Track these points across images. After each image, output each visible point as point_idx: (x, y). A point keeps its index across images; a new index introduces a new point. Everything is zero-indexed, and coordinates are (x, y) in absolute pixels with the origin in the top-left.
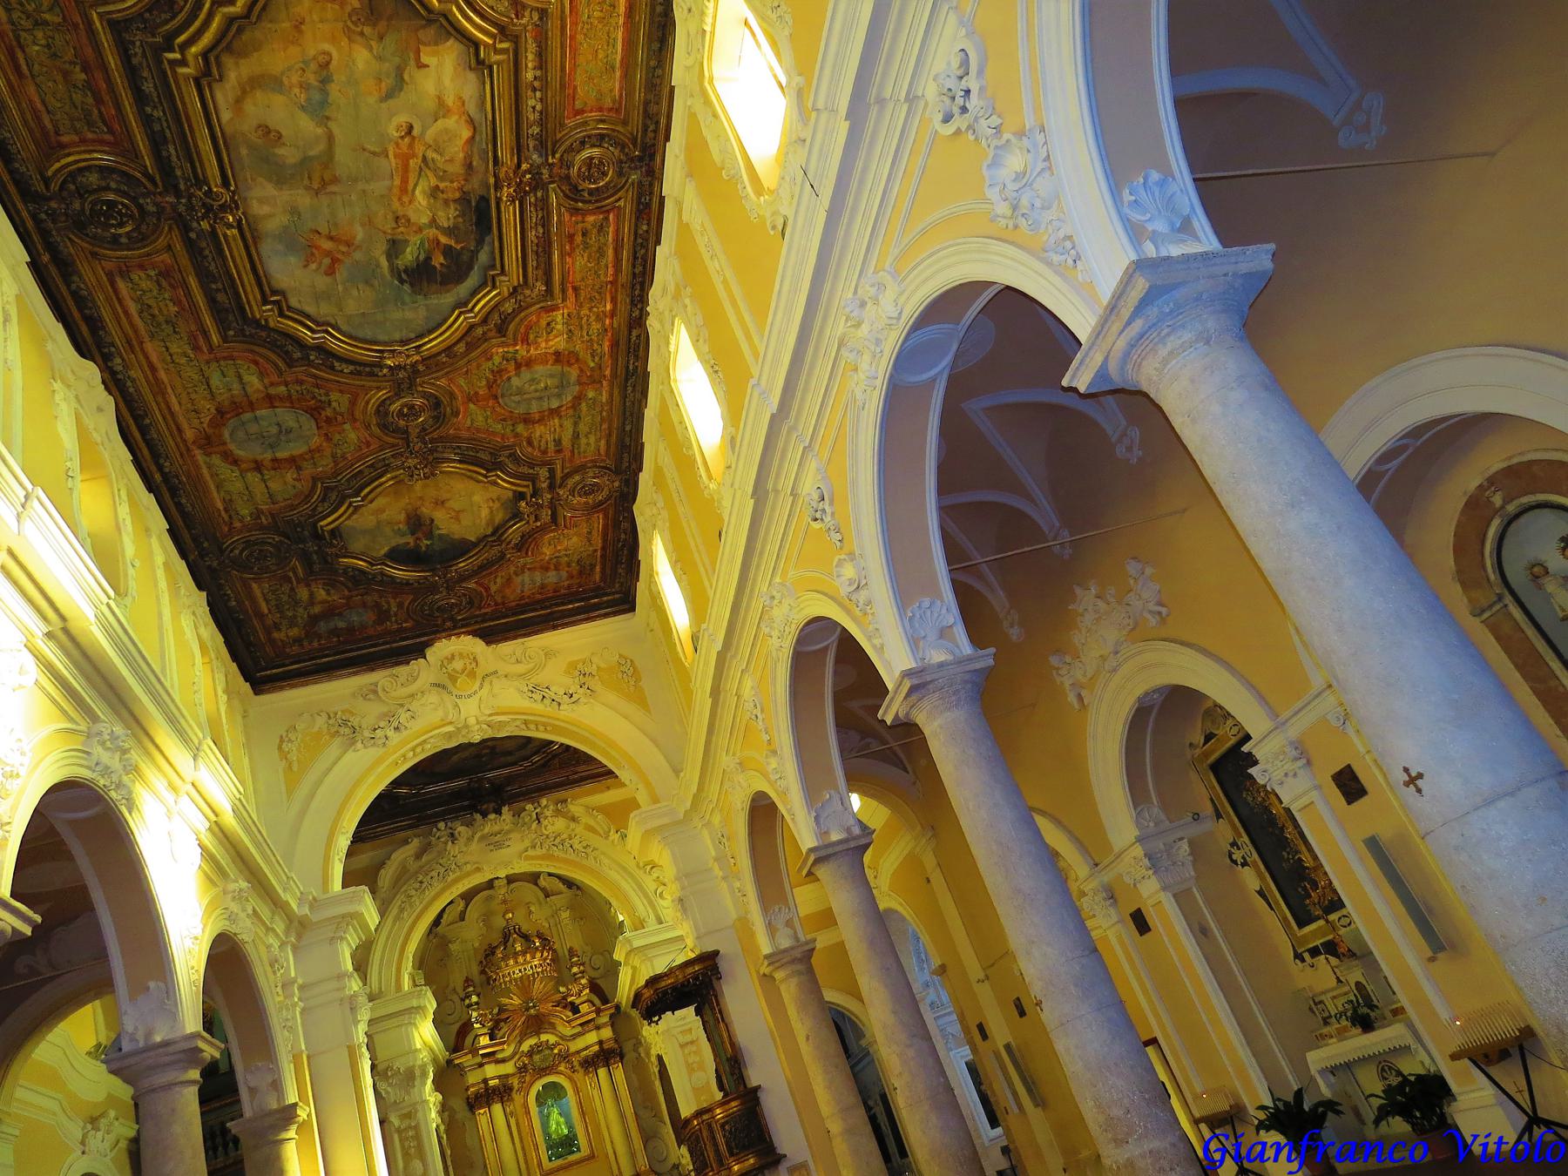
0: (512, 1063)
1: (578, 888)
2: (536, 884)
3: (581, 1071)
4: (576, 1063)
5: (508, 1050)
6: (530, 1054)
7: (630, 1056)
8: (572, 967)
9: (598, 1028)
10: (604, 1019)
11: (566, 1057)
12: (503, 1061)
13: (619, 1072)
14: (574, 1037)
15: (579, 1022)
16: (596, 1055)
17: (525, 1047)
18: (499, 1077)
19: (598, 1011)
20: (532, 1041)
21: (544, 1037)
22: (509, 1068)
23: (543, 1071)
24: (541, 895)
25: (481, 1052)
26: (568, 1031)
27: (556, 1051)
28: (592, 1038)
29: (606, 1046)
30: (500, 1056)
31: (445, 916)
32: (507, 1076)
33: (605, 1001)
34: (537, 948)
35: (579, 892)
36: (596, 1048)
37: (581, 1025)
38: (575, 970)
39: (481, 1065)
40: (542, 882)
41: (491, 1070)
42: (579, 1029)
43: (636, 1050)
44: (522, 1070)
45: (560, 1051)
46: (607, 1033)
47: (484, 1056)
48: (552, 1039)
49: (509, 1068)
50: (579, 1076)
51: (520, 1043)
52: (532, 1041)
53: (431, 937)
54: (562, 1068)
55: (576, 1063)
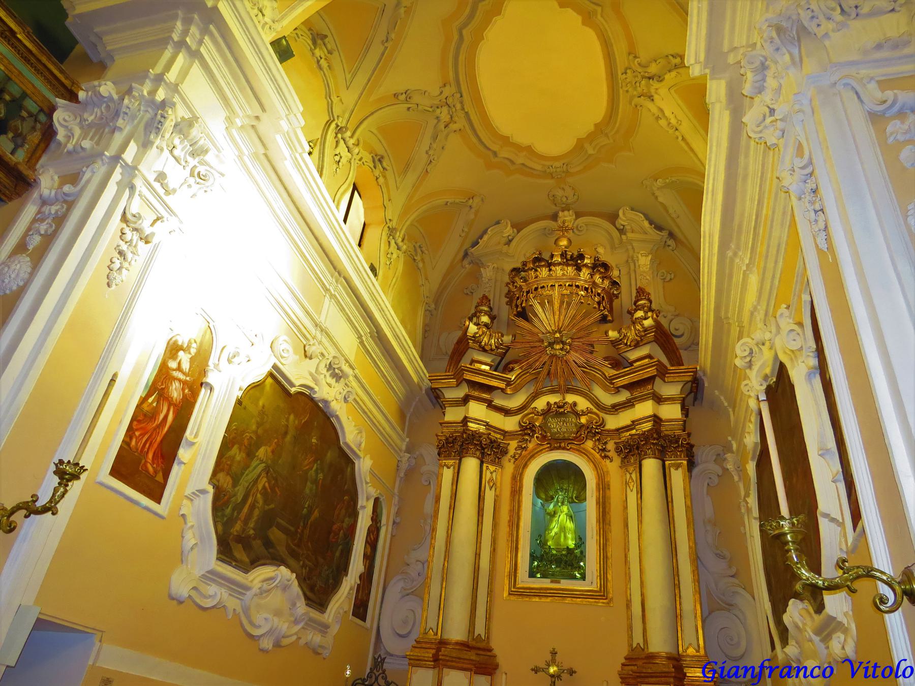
0: (519, 417)
1: (671, 235)
2: (615, 225)
3: (617, 460)
4: (611, 446)
5: (515, 402)
6: (547, 412)
7: (703, 454)
8: (636, 310)
9: (659, 400)
10: (671, 390)
11: (596, 431)
12: (506, 412)
13: (678, 477)
14: (616, 408)
15: (625, 380)
16: (646, 436)
17: (540, 404)
18: (487, 424)
19: (662, 373)
20: (553, 399)
21: (570, 398)
22: (510, 424)
23: (556, 443)
24: (615, 233)
25: (468, 376)
26: (608, 399)
27: (583, 420)
28: (645, 409)
29: (665, 430)
30: (498, 402)
31: (486, 238)
32: (504, 433)
33: (675, 357)
34: (586, 265)
35: (671, 242)
36: (647, 426)
37: (630, 387)
38: (640, 314)
39: (466, 400)
40: (622, 221)
41: (477, 410)
42: (624, 396)
43: (719, 459)
44: (527, 430)
45: (590, 422)
46: (671, 412)
47: (472, 384)
48: (583, 404)
49: (510, 424)
50: (613, 466)
51: (535, 396)
52: (553, 399)
53: (466, 262)
54: (589, 444)
55: (611, 446)
